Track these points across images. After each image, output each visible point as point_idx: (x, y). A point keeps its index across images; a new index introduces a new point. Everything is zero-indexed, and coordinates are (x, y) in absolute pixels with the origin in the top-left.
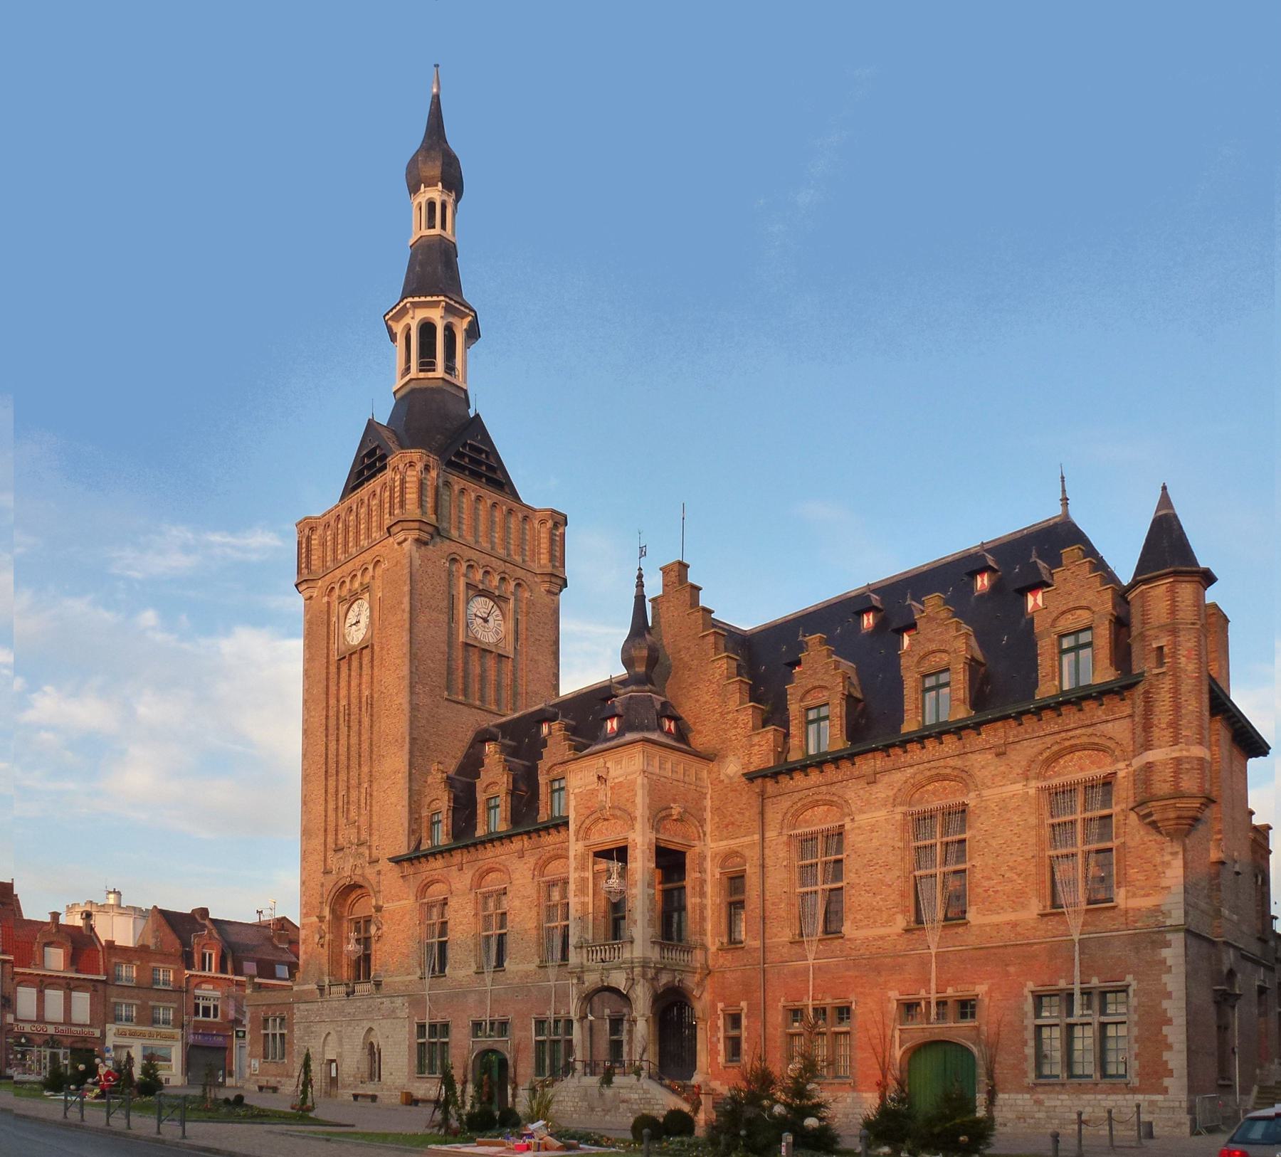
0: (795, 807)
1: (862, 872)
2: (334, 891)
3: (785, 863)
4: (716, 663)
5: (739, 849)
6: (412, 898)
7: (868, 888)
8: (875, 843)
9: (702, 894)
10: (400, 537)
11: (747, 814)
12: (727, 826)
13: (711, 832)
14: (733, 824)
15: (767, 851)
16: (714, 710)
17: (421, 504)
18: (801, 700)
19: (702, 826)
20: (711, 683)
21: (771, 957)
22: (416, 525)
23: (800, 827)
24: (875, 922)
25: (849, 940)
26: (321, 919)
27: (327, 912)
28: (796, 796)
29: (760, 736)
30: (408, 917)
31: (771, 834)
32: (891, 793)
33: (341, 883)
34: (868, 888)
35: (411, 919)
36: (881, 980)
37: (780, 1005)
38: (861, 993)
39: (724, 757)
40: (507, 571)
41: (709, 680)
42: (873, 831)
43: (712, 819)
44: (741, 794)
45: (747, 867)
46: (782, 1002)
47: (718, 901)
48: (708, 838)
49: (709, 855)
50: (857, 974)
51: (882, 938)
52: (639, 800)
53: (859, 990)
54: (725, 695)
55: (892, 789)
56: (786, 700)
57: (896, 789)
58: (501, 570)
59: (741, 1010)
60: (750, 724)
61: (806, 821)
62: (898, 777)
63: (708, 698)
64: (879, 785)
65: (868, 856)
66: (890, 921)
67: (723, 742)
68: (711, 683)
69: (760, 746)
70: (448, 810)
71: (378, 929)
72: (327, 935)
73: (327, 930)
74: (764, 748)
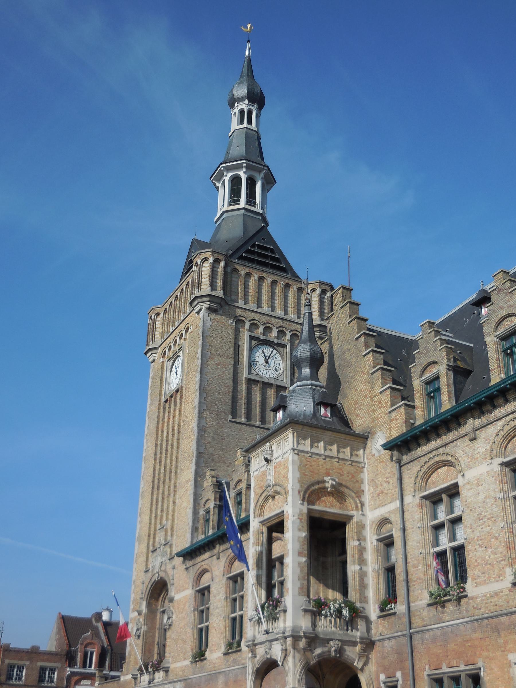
0: (423, 471)
1: (475, 526)
2: (150, 586)
3: (419, 525)
4: (366, 357)
5: (387, 516)
6: (191, 587)
7: (480, 542)
8: (482, 497)
9: (362, 562)
10: (197, 309)
11: (391, 482)
12: (379, 494)
13: (369, 502)
14: (382, 492)
15: (406, 515)
16: (366, 396)
17: (213, 285)
18: (421, 375)
19: (359, 497)
20: (364, 374)
21: (417, 622)
22: (208, 299)
23: (430, 488)
24: (489, 577)
25: (472, 598)
26: (140, 614)
27: (144, 608)
28: (423, 459)
29: (395, 412)
30: (187, 604)
31: (408, 499)
32: (488, 447)
33: (153, 580)
34: (480, 542)
35: (189, 606)
36: (501, 641)
37: (426, 673)
38: (487, 657)
39: (375, 433)
40: (284, 325)
41: (363, 372)
42: (478, 485)
43: (369, 490)
44: (386, 465)
45: (394, 532)
46: (427, 671)
47: (376, 568)
48: (367, 508)
49: (368, 523)
50: (482, 636)
51: (496, 594)
52: (290, 475)
53: (485, 654)
54: (373, 382)
55: (489, 443)
56: (411, 378)
57: (491, 442)
58: (279, 325)
59: (397, 681)
60: (389, 403)
61: (433, 483)
62: (492, 430)
63: (362, 386)
64: (479, 441)
65: (478, 509)
66: (501, 576)
67: (373, 422)
68: (364, 374)
69: (397, 420)
70: (214, 507)
71: (169, 618)
72: (143, 627)
73: (143, 622)
74: (399, 421)
